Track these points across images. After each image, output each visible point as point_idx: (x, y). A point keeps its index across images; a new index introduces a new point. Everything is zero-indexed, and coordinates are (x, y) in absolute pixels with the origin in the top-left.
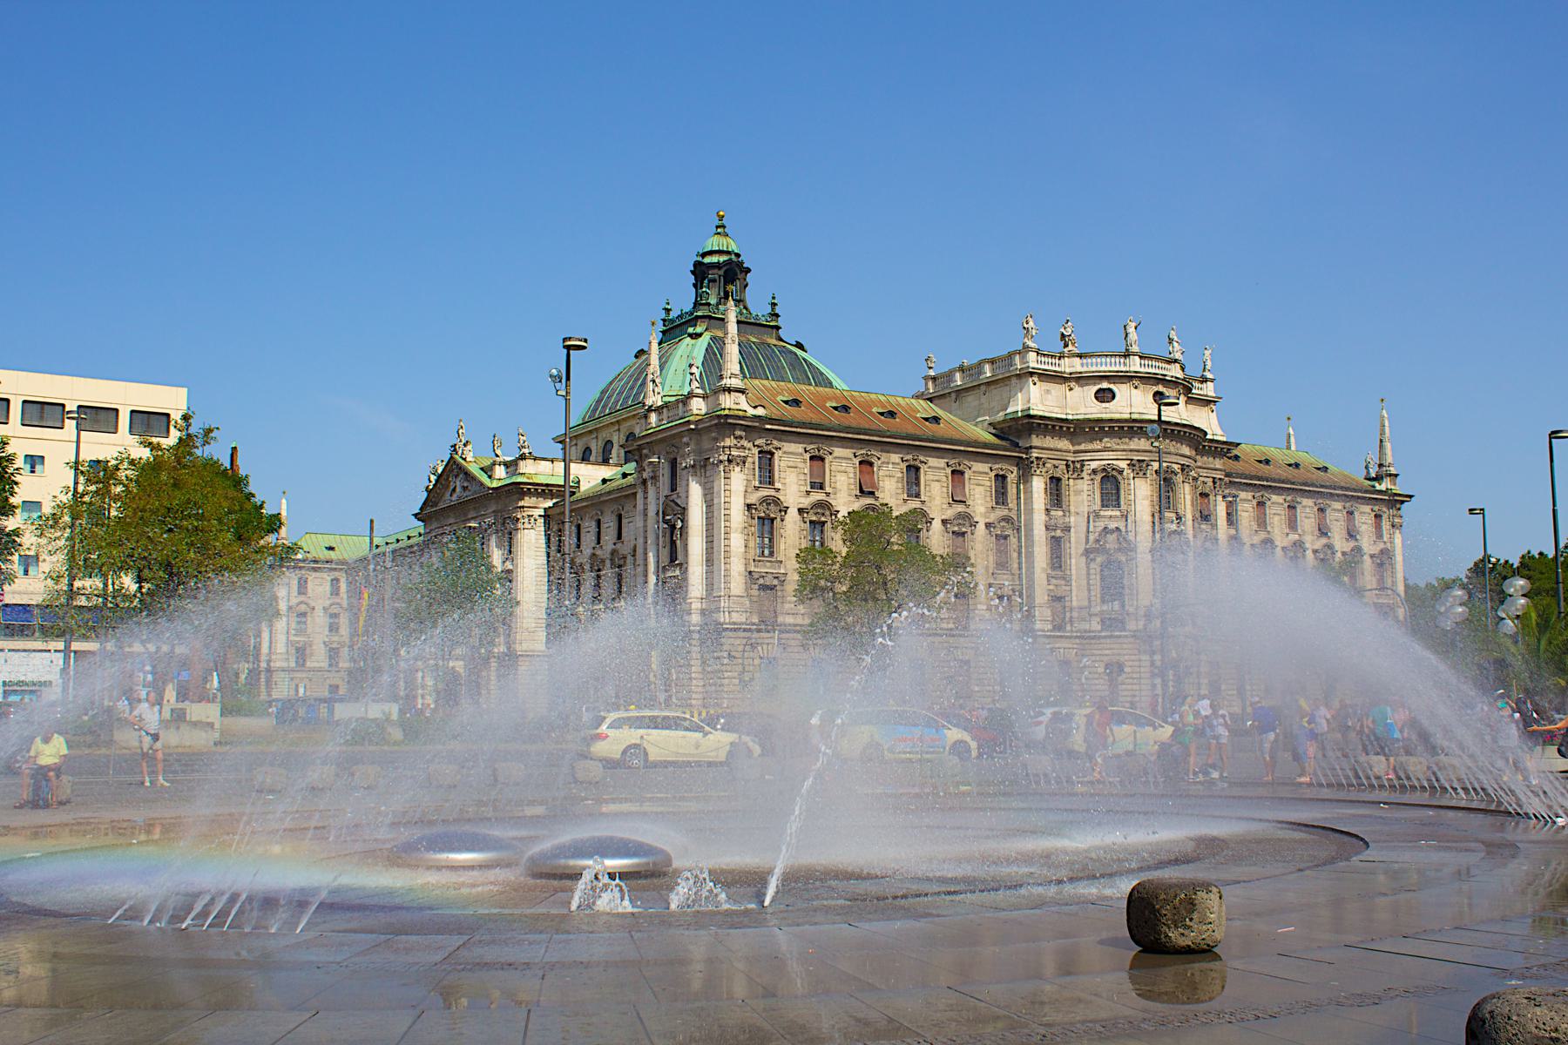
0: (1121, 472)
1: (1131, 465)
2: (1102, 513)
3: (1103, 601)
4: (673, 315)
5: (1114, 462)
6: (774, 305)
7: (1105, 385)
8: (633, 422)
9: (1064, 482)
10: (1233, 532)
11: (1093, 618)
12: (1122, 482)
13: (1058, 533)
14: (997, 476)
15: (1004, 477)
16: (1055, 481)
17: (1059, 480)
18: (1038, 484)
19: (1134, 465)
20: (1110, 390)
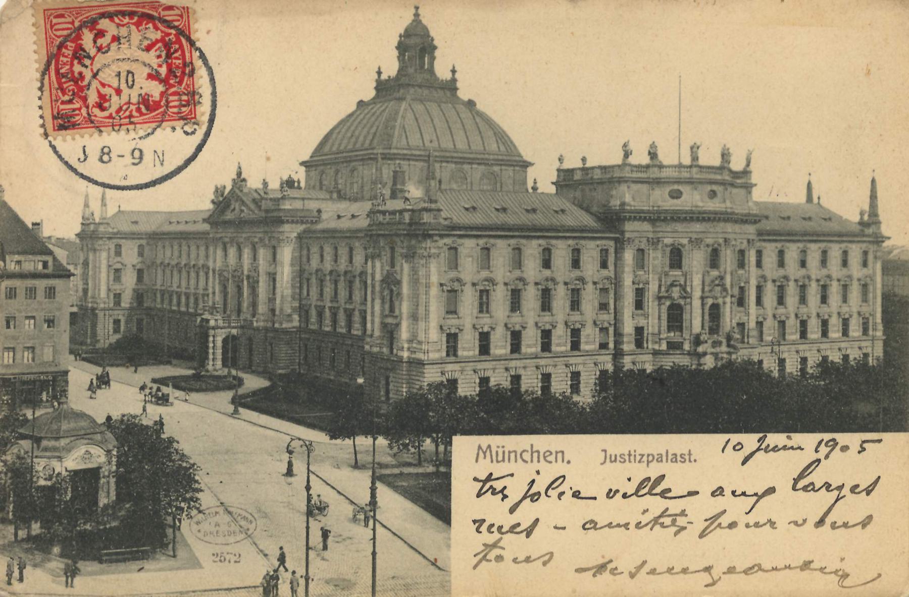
0: (683, 246)
1: (690, 241)
2: (671, 273)
3: (669, 330)
4: (384, 77)
5: (680, 240)
6: (454, 71)
7: (676, 187)
8: (357, 163)
9: (647, 251)
10: (760, 272)
11: (662, 341)
12: (684, 252)
13: (641, 286)
14: (601, 250)
15: (607, 250)
16: (641, 251)
17: (642, 250)
18: (629, 256)
19: (692, 242)
20: (679, 190)
